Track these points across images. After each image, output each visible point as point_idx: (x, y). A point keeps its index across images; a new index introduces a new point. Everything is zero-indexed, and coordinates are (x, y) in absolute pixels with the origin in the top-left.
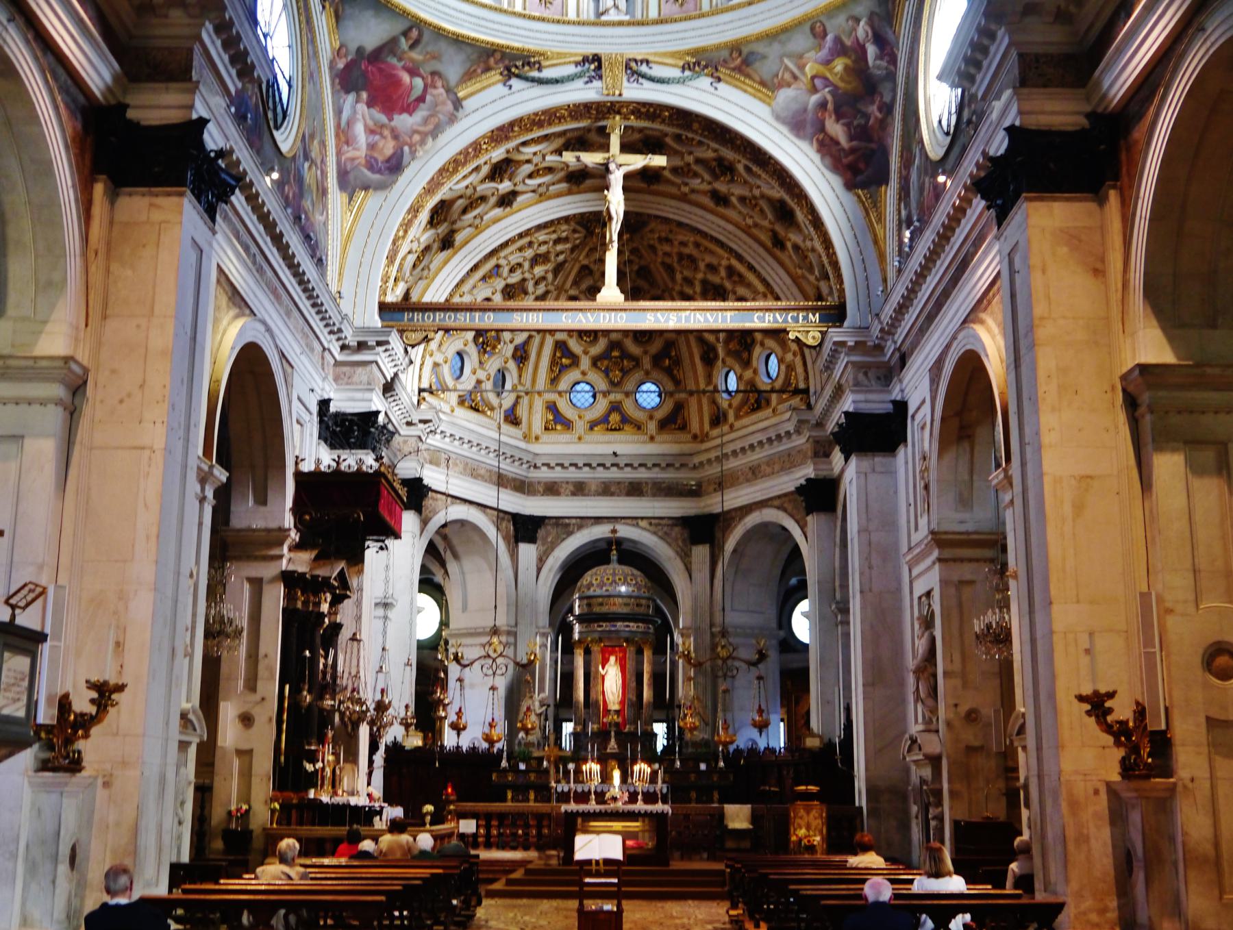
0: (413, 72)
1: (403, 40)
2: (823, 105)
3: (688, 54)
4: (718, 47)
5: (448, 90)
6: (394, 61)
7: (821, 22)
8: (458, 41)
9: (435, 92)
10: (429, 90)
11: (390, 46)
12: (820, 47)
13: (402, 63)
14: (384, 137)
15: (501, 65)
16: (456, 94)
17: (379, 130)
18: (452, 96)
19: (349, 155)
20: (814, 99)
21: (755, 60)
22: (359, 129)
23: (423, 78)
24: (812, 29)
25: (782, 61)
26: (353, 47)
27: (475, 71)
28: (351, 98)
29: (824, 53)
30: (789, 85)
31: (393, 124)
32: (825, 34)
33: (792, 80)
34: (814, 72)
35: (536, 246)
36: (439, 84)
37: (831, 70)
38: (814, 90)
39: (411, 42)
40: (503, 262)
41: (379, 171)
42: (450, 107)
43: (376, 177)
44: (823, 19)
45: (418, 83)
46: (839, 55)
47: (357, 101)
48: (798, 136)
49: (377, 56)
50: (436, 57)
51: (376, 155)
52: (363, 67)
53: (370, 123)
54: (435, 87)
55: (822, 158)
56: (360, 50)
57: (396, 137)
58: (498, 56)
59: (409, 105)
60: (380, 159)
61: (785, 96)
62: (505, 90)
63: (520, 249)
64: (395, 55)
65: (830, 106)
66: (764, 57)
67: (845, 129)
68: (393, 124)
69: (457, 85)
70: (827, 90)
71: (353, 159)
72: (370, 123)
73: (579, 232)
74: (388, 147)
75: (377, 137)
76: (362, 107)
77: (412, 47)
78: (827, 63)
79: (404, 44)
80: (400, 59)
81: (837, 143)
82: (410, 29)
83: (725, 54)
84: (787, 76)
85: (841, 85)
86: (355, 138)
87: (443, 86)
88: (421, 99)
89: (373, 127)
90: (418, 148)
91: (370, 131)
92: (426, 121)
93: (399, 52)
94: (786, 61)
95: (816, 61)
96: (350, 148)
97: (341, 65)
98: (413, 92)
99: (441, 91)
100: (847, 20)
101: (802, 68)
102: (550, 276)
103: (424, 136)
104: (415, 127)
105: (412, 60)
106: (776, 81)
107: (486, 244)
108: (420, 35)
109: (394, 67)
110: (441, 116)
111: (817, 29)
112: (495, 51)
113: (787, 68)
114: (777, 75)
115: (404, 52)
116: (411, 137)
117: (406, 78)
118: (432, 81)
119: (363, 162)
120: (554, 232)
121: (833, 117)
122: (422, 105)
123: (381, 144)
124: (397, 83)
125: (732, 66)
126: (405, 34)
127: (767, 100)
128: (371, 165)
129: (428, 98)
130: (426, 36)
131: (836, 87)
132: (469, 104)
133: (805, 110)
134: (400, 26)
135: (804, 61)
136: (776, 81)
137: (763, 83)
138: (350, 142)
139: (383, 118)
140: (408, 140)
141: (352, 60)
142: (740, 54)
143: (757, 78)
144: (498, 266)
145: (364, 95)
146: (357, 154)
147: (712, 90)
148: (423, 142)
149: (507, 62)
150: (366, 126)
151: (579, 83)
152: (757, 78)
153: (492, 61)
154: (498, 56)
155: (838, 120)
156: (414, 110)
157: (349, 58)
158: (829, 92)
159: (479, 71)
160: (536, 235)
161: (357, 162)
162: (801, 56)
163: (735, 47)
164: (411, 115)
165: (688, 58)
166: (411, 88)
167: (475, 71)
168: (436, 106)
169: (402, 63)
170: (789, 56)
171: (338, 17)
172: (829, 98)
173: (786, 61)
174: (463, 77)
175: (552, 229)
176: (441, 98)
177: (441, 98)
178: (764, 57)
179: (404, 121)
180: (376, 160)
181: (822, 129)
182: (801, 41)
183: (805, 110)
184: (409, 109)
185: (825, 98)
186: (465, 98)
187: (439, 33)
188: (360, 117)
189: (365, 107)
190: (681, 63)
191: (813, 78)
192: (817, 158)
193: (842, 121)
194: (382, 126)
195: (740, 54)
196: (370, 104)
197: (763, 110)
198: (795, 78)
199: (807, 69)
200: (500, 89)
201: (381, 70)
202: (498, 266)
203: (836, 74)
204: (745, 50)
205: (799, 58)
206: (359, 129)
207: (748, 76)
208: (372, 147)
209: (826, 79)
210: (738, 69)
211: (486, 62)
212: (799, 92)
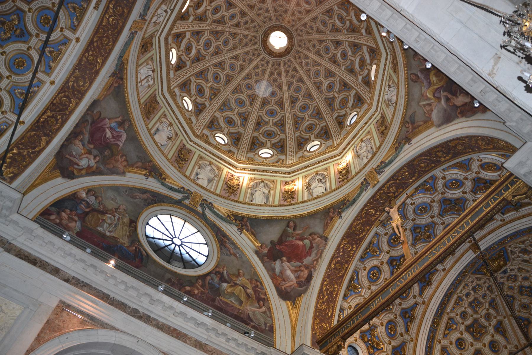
0: (302, 239)
1: (289, 229)
2: (448, 100)
3: (394, 145)
4: (400, 130)
5: (321, 237)
6: (291, 239)
7: (411, 74)
8: (312, 215)
9: (316, 241)
10: (313, 242)
11: (284, 234)
12: (422, 82)
13: (295, 238)
14: (302, 271)
15: (336, 213)
16: (324, 236)
17: (299, 269)
18: (323, 238)
19: (287, 285)
20: (443, 102)
21: (414, 118)
22: (289, 273)
23: (307, 239)
24: (412, 80)
25: (420, 106)
26: (268, 242)
27: (327, 222)
28: (278, 262)
29: (425, 83)
30: (433, 111)
31: (304, 264)
32: (417, 75)
33: (431, 107)
34: (432, 93)
35: (464, 297)
36: (316, 237)
37: (434, 85)
38: (439, 99)
39: (293, 228)
40: (453, 315)
41: (304, 285)
42: (324, 242)
43: (304, 287)
44: (410, 72)
45: (307, 241)
46: (429, 75)
47: (282, 263)
48: (451, 122)
49: (281, 241)
50: (308, 228)
51: (301, 280)
52: (278, 248)
53: (293, 268)
54: (315, 239)
55: (466, 117)
56: (272, 242)
57: (307, 267)
58: (332, 210)
59: (307, 252)
60: (303, 280)
61: (435, 116)
62: (341, 219)
63: (457, 303)
64: (290, 237)
65: (450, 96)
66: (415, 112)
67: (462, 95)
68: (304, 264)
69: (324, 233)
70: (442, 92)
71: (291, 286)
72: (293, 268)
73: (483, 278)
74: (306, 273)
75: (299, 273)
76: (286, 264)
77: (295, 229)
78: (430, 84)
79: (290, 230)
80: (293, 237)
81: (466, 104)
82: (289, 223)
83: (404, 128)
84: (428, 108)
85: (442, 83)
86: (288, 277)
87: (318, 237)
88: (311, 247)
89: (296, 269)
90: (316, 266)
91: (294, 272)
92: (317, 254)
93: (290, 235)
94: (421, 104)
95: (428, 89)
96: (287, 282)
97: (266, 251)
98: (306, 247)
99: (319, 239)
100: (415, 60)
101: (428, 99)
102: (491, 311)
103: (317, 260)
104: (314, 259)
105: (298, 234)
106: (427, 115)
107: (433, 309)
108: (295, 223)
109: (292, 242)
110: (321, 248)
111: (414, 78)
112: (329, 209)
113: (424, 105)
114: (425, 113)
115: (293, 234)
116: (313, 264)
117: (300, 243)
118: (312, 238)
119: (296, 285)
120: (467, 285)
121: (455, 98)
122: (313, 249)
123: (302, 274)
124: (298, 246)
125: (411, 130)
126: (288, 226)
127: (432, 125)
128: (300, 284)
129: (314, 245)
130: (297, 222)
131: (442, 86)
132: (329, 237)
133: (445, 110)
134: (283, 225)
135: (425, 94)
136: (427, 115)
137: (425, 122)
138: (286, 279)
139: (299, 264)
140: (312, 266)
141: (270, 248)
142: (408, 123)
143: (422, 123)
144: (450, 319)
145: (284, 259)
146: (292, 283)
147: (410, 145)
148: (317, 262)
149: (337, 210)
150: (292, 271)
151: (364, 192)
152: (422, 123)
153: (331, 214)
154: (332, 210)
155: (457, 97)
156: (311, 253)
157: (269, 247)
158: (443, 92)
159: (329, 221)
160: (458, 291)
161: (293, 286)
162: (422, 95)
163: (404, 123)
164: (310, 256)
165: (396, 146)
166: (305, 245)
167: (327, 222)
168: (319, 245)
169: (295, 238)
170: (420, 101)
171: (254, 235)
172: (445, 94)
173: (421, 104)
174: (324, 229)
175: (463, 284)
176: (319, 242)
177: (319, 242)
178: (415, 112)
179: (307, 260)
180: (302, 281)
181: (456, 107)
182: (416, 90)
183: (445, 110)
184: (309, 254)
185: (445, 96)
186: (328, 235)
187: (302, 217)
188: (287, 268)
189: (288, 263)
190: (394, 150)
191: (434, 96)
192: (464, 119)
193: (458, 95)
194: (300, 267)
195: (408, 123)
196: (289, 261)
197: (433, 129)
198: (430, 105)
199: (429, 96)
200: (339, 220)
201: (286, 245)
202: (450, 319)
203: (437, 83)
204: (407, 119)
205: (422, 96)
206: (289, 273)
207: (419, 126)
208: (297, 277)
209: (437, 89)
210: (414, 128)
211: (329, 216)
212: (437, 107)
